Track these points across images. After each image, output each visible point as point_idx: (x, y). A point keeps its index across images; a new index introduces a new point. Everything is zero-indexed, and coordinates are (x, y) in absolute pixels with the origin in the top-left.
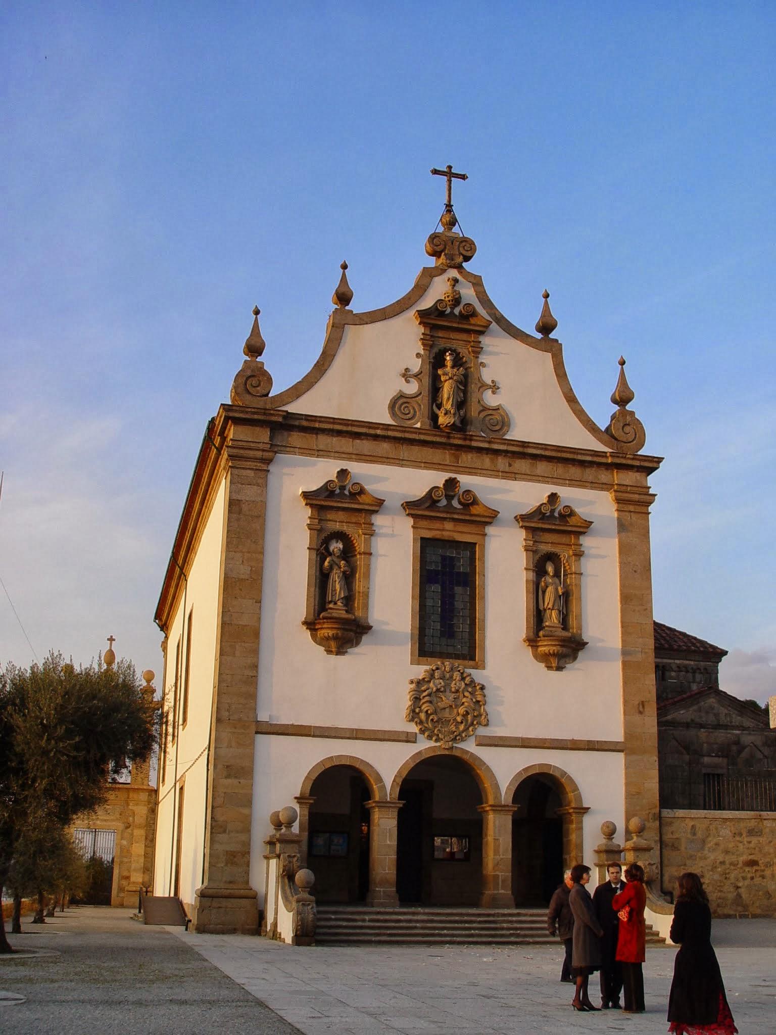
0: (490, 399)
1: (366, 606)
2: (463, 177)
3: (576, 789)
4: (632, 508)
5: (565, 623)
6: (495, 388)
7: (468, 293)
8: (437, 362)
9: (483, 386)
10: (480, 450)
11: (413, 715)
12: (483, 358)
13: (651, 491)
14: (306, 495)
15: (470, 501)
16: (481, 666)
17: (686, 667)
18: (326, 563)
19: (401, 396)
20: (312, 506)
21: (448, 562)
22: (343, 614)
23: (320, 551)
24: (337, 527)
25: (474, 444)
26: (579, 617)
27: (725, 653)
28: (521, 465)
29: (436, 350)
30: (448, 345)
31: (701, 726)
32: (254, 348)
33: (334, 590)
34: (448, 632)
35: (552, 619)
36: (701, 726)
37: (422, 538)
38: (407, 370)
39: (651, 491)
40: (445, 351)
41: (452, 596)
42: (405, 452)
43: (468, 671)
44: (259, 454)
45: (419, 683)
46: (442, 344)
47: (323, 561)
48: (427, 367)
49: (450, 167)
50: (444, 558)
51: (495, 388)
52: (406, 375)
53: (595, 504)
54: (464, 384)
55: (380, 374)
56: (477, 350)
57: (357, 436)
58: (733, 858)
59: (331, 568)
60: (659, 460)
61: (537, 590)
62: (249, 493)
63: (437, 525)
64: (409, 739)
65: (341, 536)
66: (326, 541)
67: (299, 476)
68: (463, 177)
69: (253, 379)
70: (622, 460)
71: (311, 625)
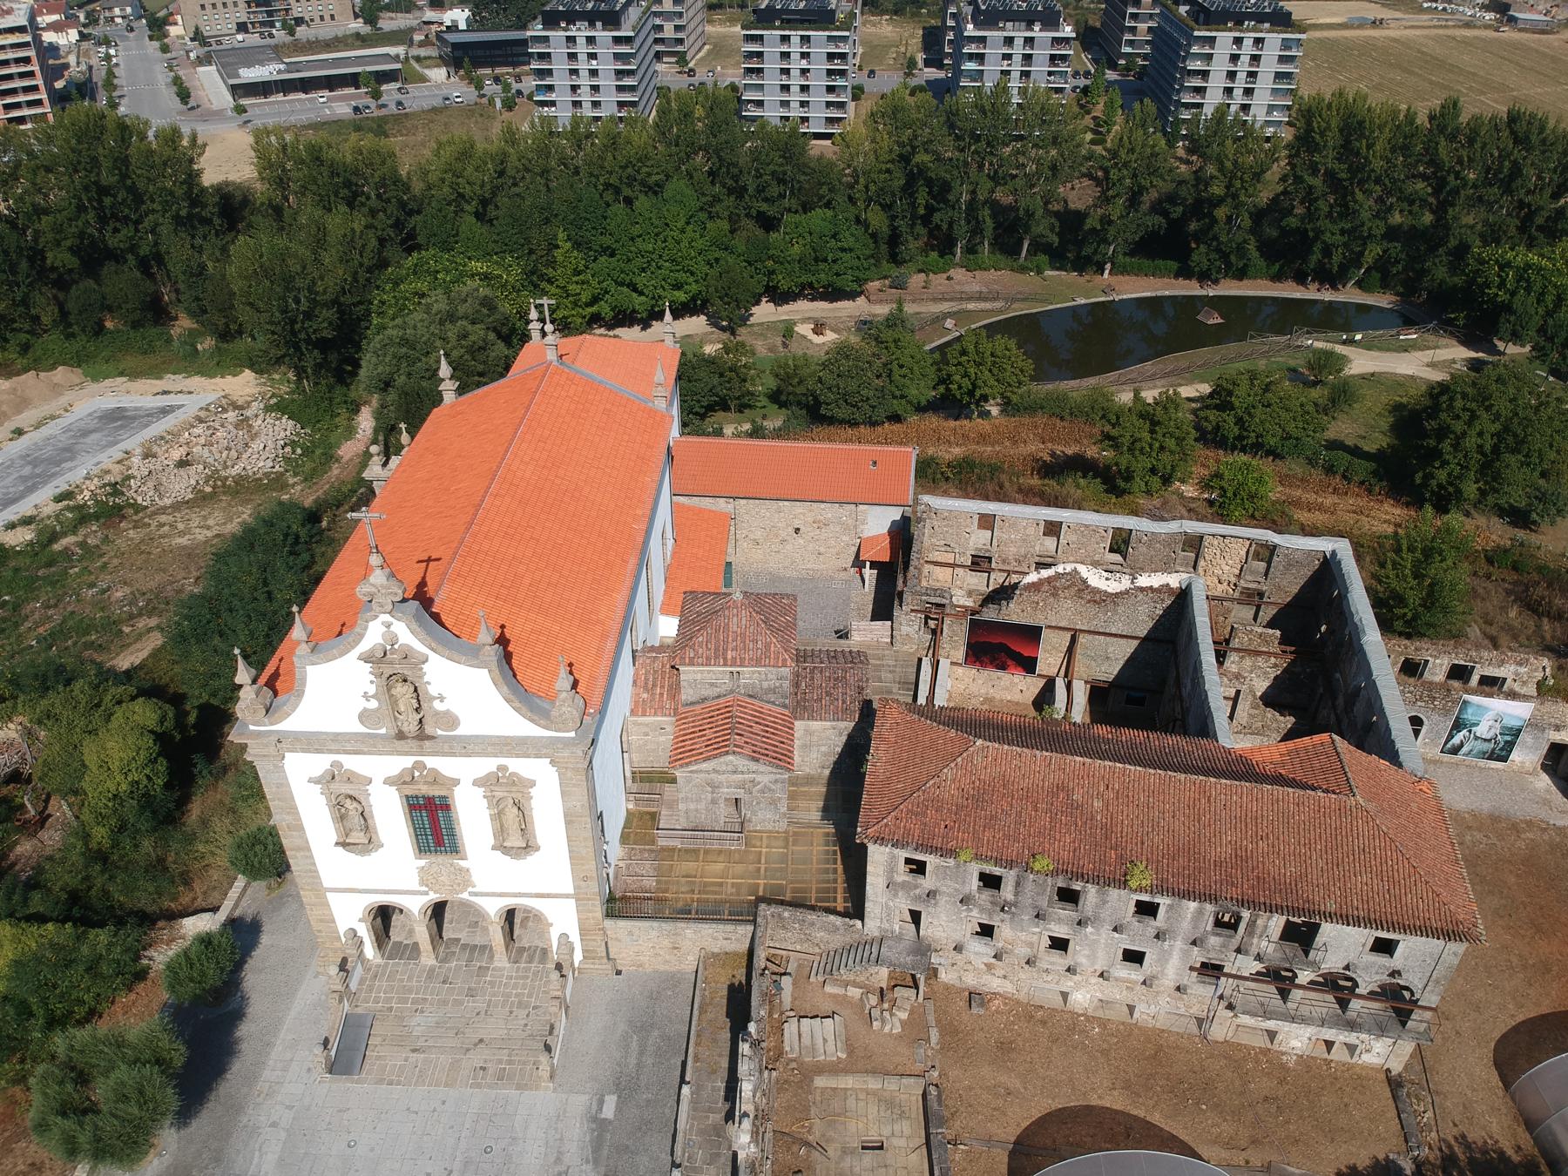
0: (438, 706)
6: (442, 699)
11: (422, 883)
19: (365, 710)
51: (442, 699)
52: (366, 696)
61: (498, 817)
64: (426, 893)
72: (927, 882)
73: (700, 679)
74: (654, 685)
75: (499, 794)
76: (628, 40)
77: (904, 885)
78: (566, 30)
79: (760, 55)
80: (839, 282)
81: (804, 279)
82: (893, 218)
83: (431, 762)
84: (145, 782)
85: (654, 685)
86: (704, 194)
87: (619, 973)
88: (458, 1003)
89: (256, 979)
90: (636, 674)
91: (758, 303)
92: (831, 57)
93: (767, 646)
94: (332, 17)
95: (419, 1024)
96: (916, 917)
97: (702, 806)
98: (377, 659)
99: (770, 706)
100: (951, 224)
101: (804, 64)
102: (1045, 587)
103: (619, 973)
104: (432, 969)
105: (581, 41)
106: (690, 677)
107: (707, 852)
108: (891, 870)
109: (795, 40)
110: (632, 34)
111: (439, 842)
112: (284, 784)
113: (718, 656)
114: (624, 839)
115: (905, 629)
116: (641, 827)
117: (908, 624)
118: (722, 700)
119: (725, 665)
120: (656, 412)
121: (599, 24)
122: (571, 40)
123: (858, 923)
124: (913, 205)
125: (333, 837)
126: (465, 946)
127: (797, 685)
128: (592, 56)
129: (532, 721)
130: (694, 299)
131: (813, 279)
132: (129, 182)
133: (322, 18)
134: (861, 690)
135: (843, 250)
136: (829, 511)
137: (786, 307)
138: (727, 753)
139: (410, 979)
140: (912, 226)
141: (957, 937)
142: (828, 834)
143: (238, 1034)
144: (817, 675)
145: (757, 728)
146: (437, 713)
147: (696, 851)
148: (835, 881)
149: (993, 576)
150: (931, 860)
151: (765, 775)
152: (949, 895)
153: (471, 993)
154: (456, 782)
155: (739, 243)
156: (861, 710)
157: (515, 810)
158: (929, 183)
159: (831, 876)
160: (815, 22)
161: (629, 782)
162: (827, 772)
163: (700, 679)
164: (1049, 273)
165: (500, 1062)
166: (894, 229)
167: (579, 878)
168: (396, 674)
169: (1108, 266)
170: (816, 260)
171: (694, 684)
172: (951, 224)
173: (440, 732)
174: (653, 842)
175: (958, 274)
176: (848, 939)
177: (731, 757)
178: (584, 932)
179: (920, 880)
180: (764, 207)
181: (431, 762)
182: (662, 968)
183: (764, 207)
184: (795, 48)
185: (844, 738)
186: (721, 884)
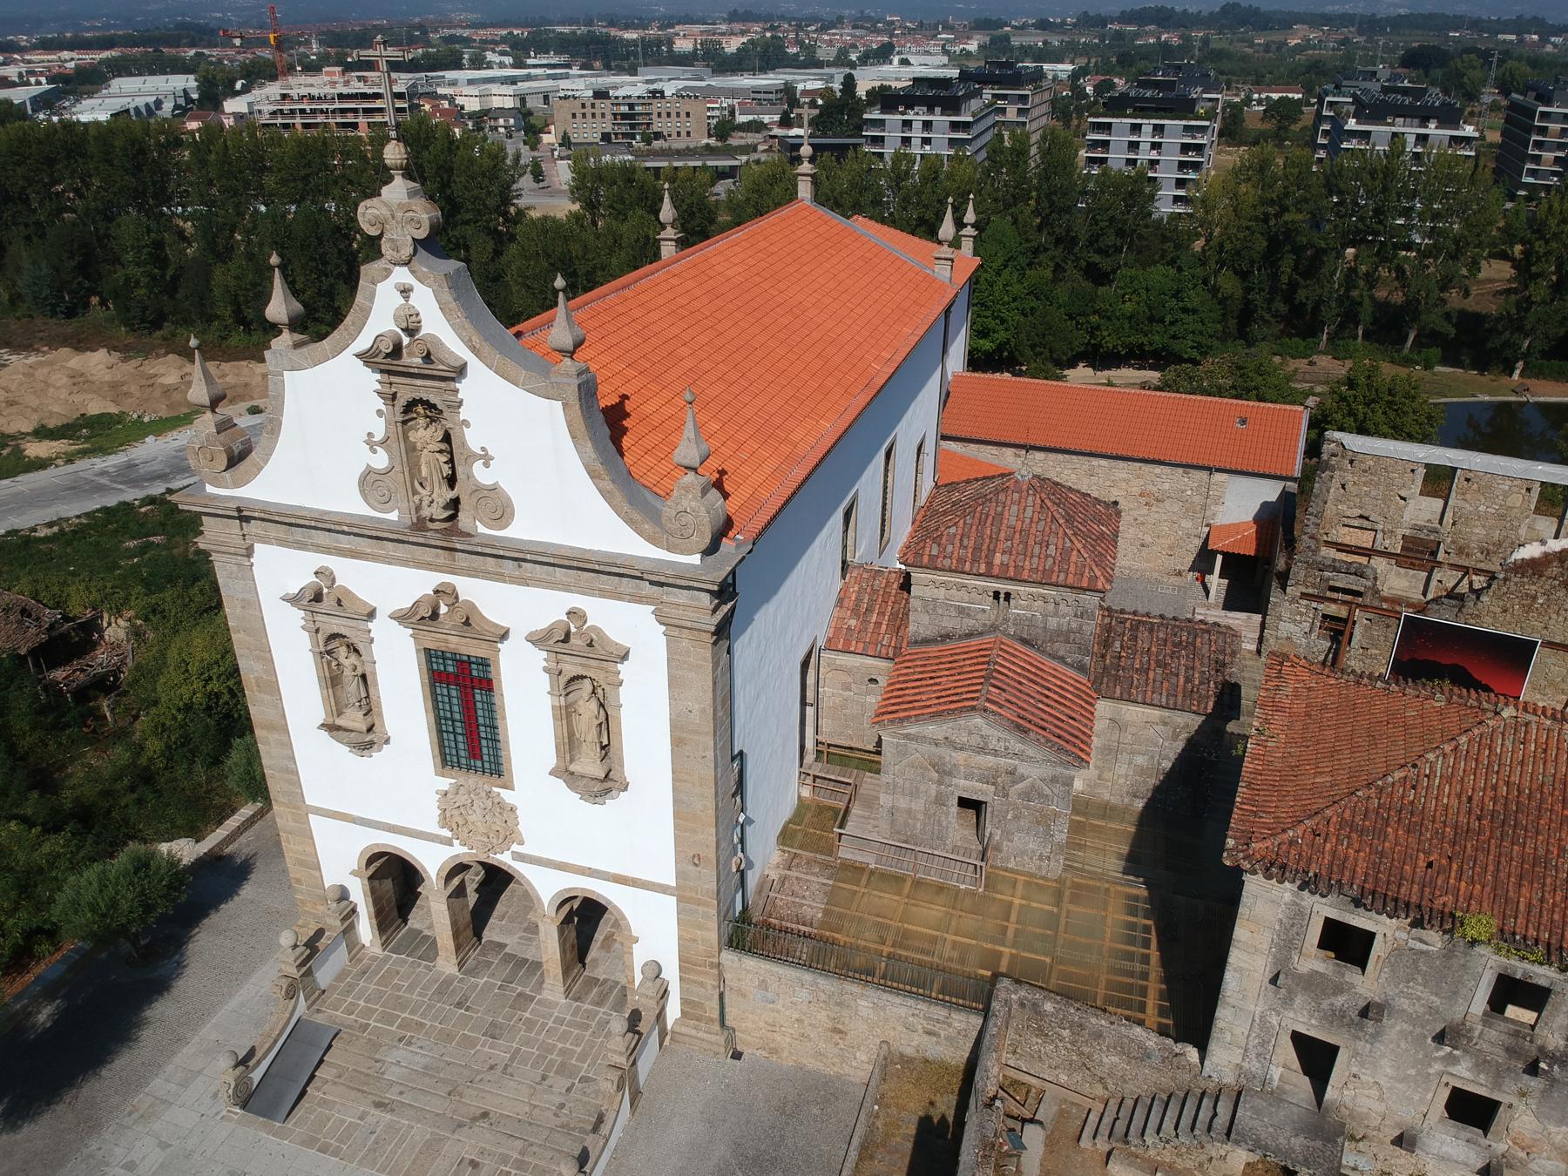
0: (482, 475)
11: (444, 821)
12: (464, 414)
16: (509, 786)
19: (369, 471)
24: (336, 630)
29: (401, 402)
30: (417, 395)
37: (427, 651)
43: (496, 789)
51: (487, 459)
52: (371, 444)
53: (628, 623)
61: (565, 715)
64: (448, 842)
72: (1367, 984)
73: (947, 599)
74: (869, 610)
75: (571, 669)
76: (965, 126)
77: (1311, 983)
78: (903, 113)
79: (1105, 144)
80: (1176, 346)
81: (1135, 339)
82: (1248, 290)
83: (472, 589)
84: (226, 697)
85: (869, 610)
86: (1027, 241)
87: (737, 1056)
88: (468, 1042)
89: (209, 943)
90: (844, 591)
91: (1073, 365)
92: (1185, 148)
93: (1065, 554)
94: (688, 134)
95: (400, 1061)
96: (1316, 1059)
97: (918, 805)
98: (385, 358)
99: (1054, 664)
100: (1316, 308)
101: (1154, 155)
102: (1554, 569)
103: (737, 1056)
104: (449, 981)
105: (917, 126)
106: (929, 593)
107: (918, 884)
108: (1288, 944)
109: (1147, 129)
110: (970, 119)
111: (475, 752)
112: (253, 603)
113: (978, 562)
114: (785, 837)
115: (1286, 628)
116: (814, 829)
117: (1293, 621)
118: (974, 641)
119: (988, 575)
120: (935, 279)
121: (938, 110)
122: (907, 124)
123: (1192, 1054)
124: (1275, 277)
125: (319, 714)
126: (509, 958)
127: (1106, 644)
128: (926, 141)
129: (630, 522)
130: (1000, 348)
131: (1145, 340)
132: (449, 192)
133: (679, 134)
134: (1220, 666)
135: (1185, 310)
136: (1166, 479)
137: (1106, 373)
138: (973, 708)
139: (411, 989)
140: (1270, 301)
141: (1407, 1115)
142: (1130, 897)
143: (148, 1013)
144: (1143, 635)
145: (1030, 688)
146: (478, 488)
147: (899, 879)
148: (1145, 976)
149: (1437, 575)
150: (1386, 930)
151: (1035, 764)
152: (1413, 1020)
153: (493, 1032)
154: (504, 636)
155: (1062, 293)
156: (1220, 697)
157: (593, 705)
158: (1298, 250)
159: (1138, 967)
160: (1171, 110)
161: (810, 757)
162: (1139, 805)
163: (947, 599)
164: (1439, 369)
165: (505, 1159)
166: (1248, 303)
167: (687, 859)
168: (417, 391)
169: (1520, 364)
170: (1151, 319)
171: (931, 606)
172: (1316, 308)
173: (482, 529)
174: (830, 850)
175: (1324, 361)
176: (1166, 1081)
177: (978, 720)
178: (686, 964)
179: (1352, 975)
180: (1096, 258)
181: (472, 589)
182: (812, 1064)
183: (1096, 258)
184: (1146, 138)
185: (1180, 746)
186: (934, 940)
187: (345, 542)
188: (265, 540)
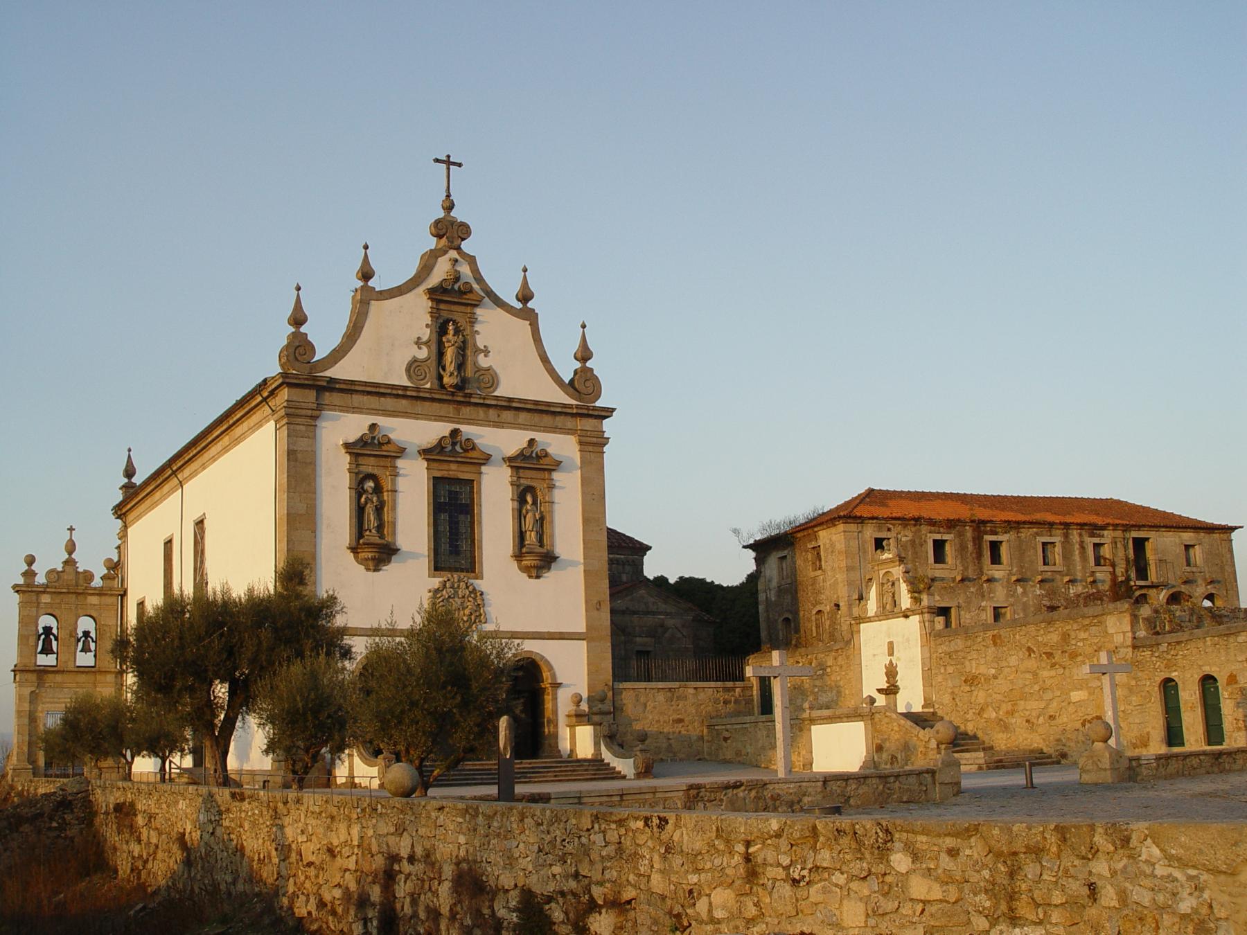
0: (483, 361)
1: (394, 533)
2: (460, 165)
3: (551, 668)
4: (591, 448)
5: (541, 541)
6: (486, 352)
7: (465, 269)
8: (442, 331)
9: (477, 351)
10: (476, 404)
12: (477, 327)
13: (606, 435)
14: (347, 446)
15: (470, 446)
16: (480, 577)
17: (617, 560)
18: (363, 500)
19: (415, 360)
20: (350, 453)
21: (453, 496)
22: (377, 540)
23: (358, 490)
24: (370, 470)
25: (473, 400)
26: (552, 536)
27: (649, 548)
28: (507, 415)
31: (634, 613)
32: (298, 319)
33: (369, 521)
34: (455, 550)
35: (531, 538)
36: (634, 613)
38: (419, 338)
39: (606, 435)
40: (447, 321)
41: (457, 523)
42: (420, 407)
44: (309, 413)
45: (436, 591)
46: (445, 315)
47: (360, 497)
48: (435, 336)
49: (449, 156)
50: (450, 492)
51: (486, 352)
52: (418, 342)
53: (562, 446)
54: (462, 349)
55: (396, 343)
56: (473, 321)
57: (383, 395)
58: (666, 718)
59: (366, 503)
60: (614, 410)
61: (520, 516)
62: (302, 444)
63: (445, 466)
65: (372, 477)
66: (361, 482)
67: (340, 429)
68: (460, 165)
69: (298, 348)
70: (582, 408)
71: (354, 549)
187: (389, 403)
188: (333, 407)
